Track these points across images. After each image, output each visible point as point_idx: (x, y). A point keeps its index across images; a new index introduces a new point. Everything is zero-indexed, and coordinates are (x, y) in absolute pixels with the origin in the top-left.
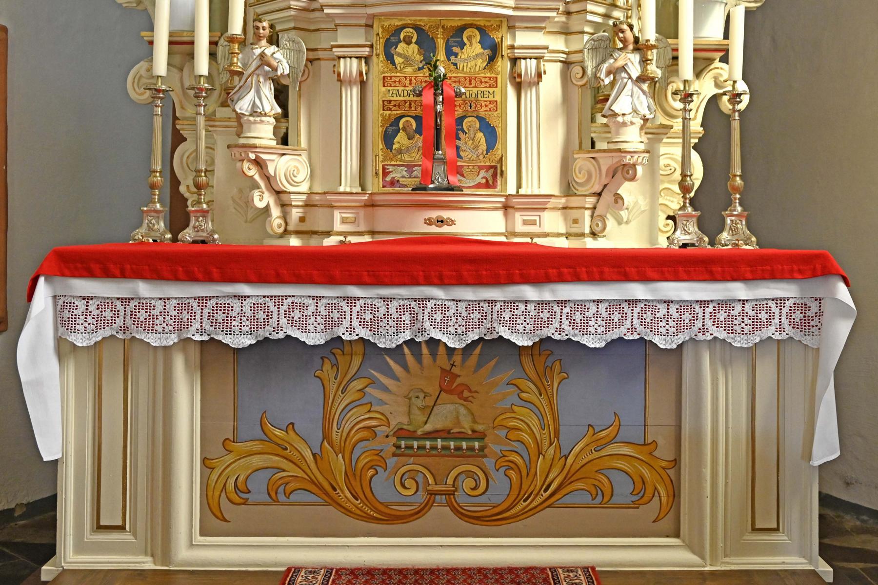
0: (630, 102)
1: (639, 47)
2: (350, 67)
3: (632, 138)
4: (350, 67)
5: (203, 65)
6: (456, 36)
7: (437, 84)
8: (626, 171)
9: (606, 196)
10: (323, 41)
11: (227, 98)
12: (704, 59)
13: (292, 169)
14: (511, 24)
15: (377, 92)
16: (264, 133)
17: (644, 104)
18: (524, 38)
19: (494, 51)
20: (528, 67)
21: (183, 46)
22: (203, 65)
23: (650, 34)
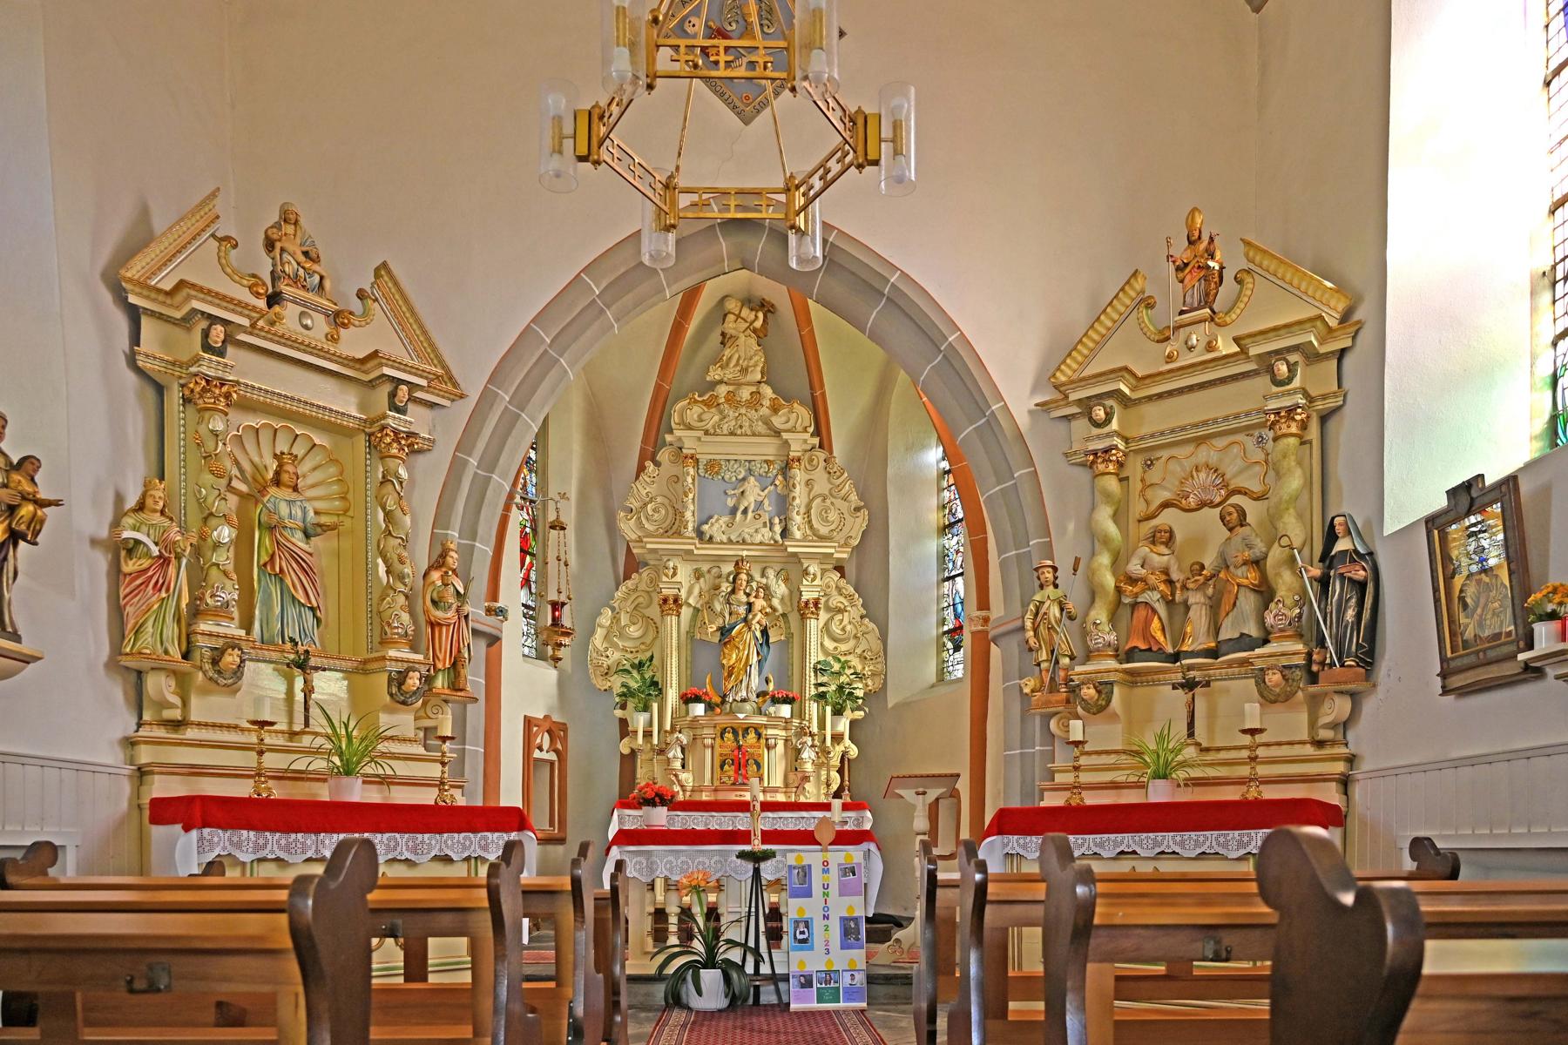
0: (808, 754)
1: (812, 735)
2: (708, 741)
3: (809, 767)
4: (708, 741)
5: (655, 741)
6: (746, 731)
7: (739, 747)
8: (806, 779)
9: (800, 788)
10: (698, 732)
11: (662, 752)
12: (837, 738)
13: (687, 777)
14: (766, 727)
15: (718, 750)
16: (677, 765)
17: (813, 755)
18: (770, 732)
19: (759, 736)
20: (772, 742)
21: (648, 734)
22: (655, 741)
23: (815, 729)
